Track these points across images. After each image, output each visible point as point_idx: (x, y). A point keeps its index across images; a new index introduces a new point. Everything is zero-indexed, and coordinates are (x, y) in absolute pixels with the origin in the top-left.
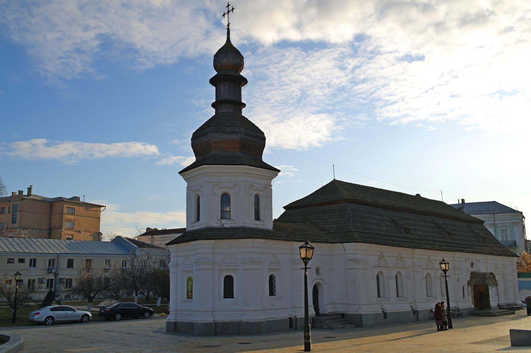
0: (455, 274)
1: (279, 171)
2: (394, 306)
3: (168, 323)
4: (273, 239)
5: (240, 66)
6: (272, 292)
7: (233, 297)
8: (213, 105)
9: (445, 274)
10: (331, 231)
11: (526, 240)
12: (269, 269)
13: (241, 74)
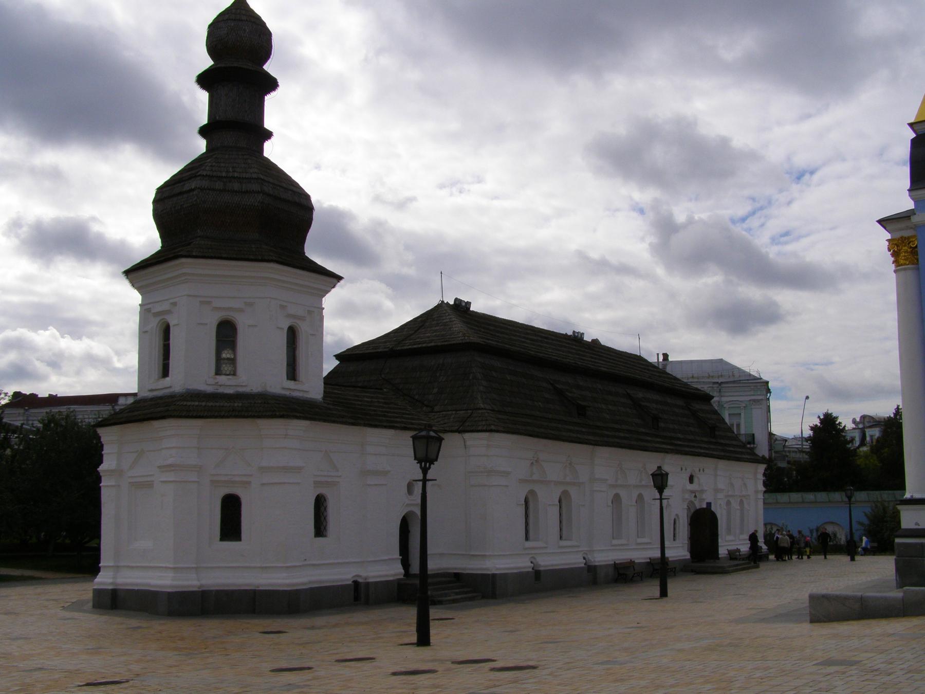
1: (339, 278)
2: (557, 556)
3: (98, 593)
4: (325, 421)
6: (320, 529)
7: (240, 540)
8: (204, 131)
10: (437, 408)
11: (771, 435)
12: (315, 482)
13: (266, 67)
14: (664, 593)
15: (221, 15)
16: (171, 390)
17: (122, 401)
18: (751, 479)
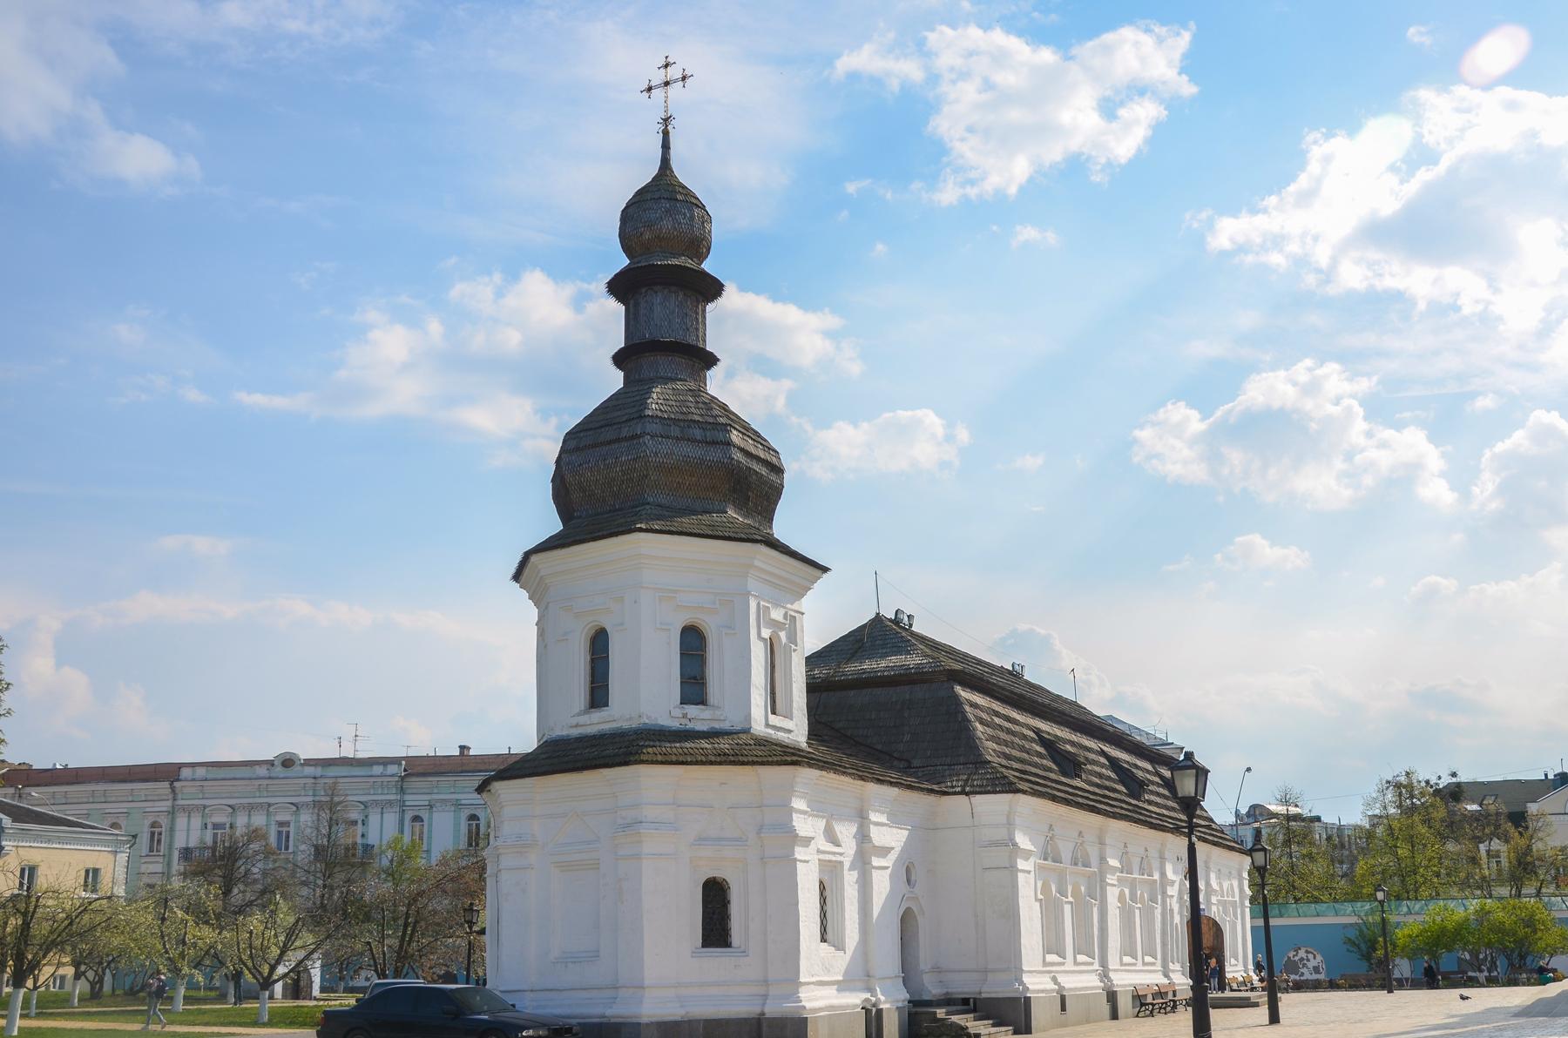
1: (825, 570)
5: (699, 246)
10: (916, 763)
14: (1274, 1018)
15: (640, 193)
16: (614, 725)
17: (185, 773)
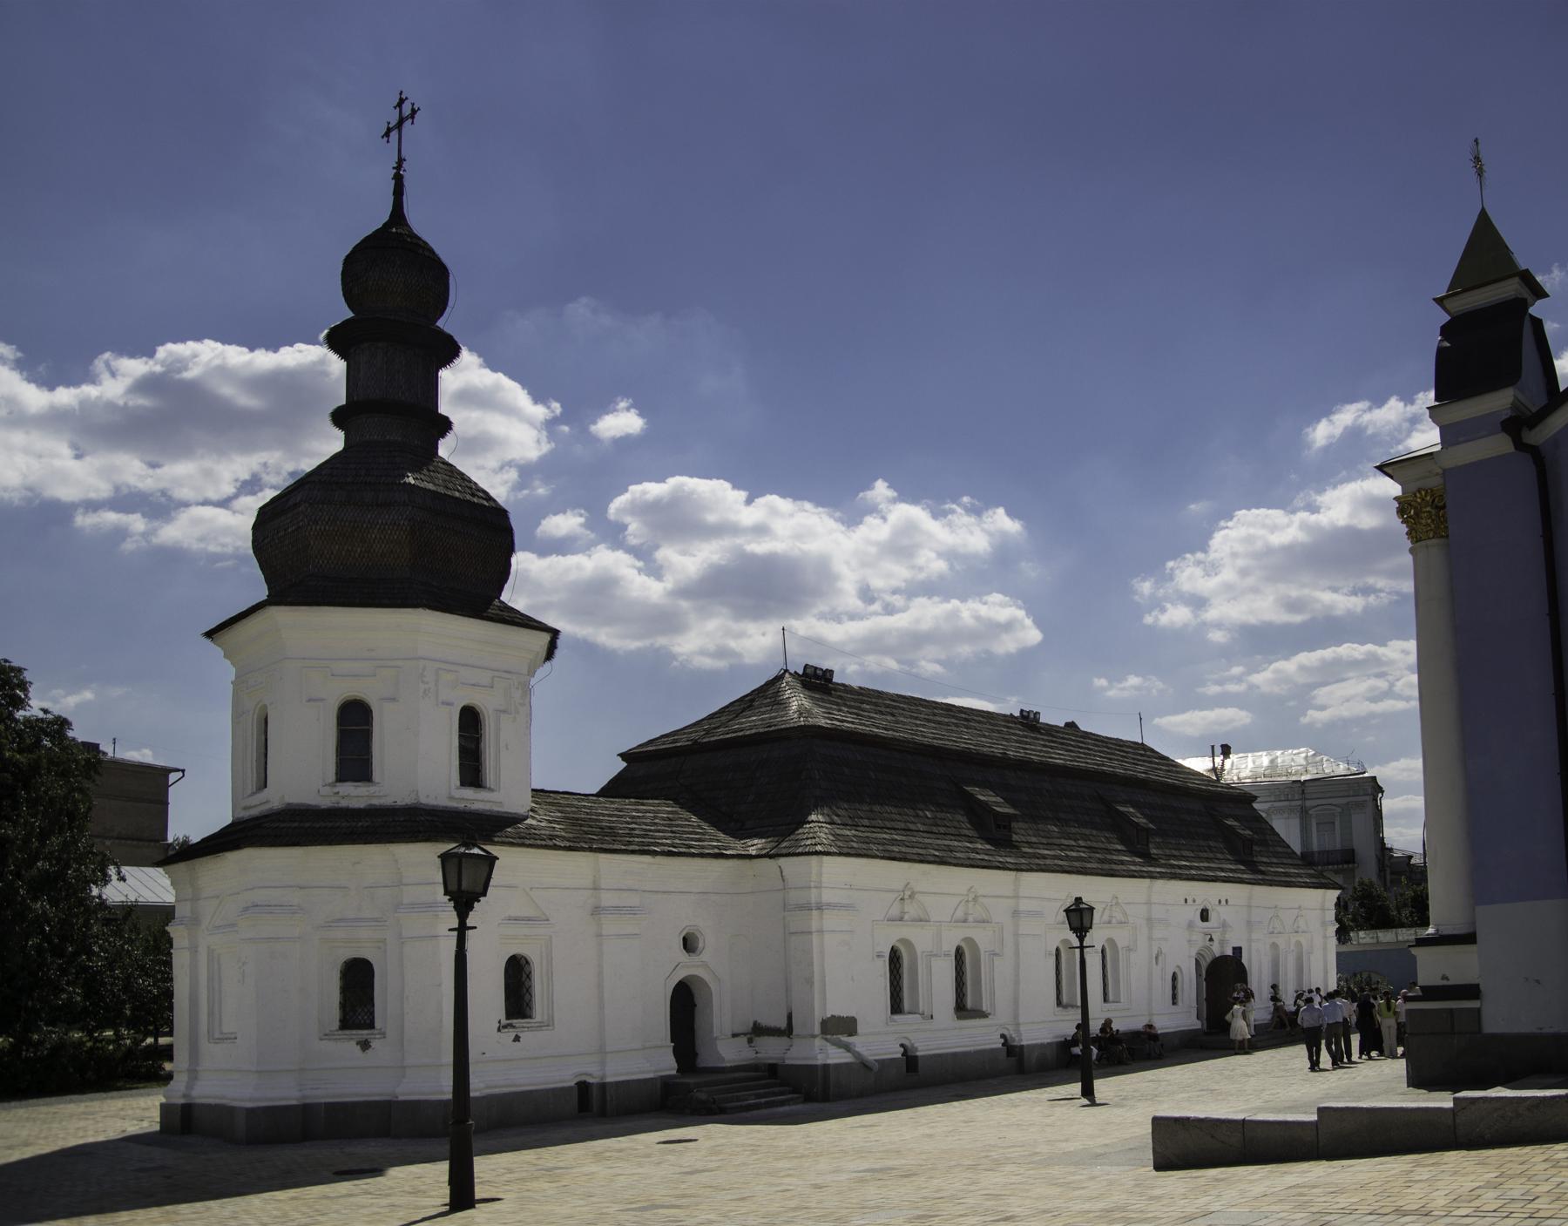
0: (1150, 938)
9: (1081, 939)
18: (1313, 909)
